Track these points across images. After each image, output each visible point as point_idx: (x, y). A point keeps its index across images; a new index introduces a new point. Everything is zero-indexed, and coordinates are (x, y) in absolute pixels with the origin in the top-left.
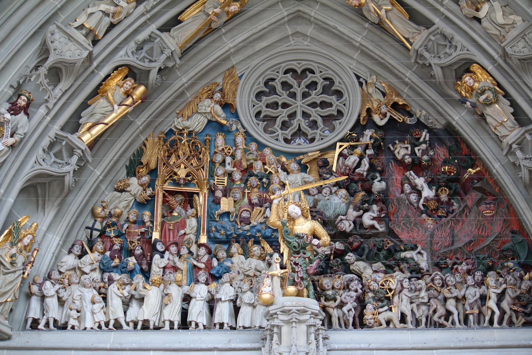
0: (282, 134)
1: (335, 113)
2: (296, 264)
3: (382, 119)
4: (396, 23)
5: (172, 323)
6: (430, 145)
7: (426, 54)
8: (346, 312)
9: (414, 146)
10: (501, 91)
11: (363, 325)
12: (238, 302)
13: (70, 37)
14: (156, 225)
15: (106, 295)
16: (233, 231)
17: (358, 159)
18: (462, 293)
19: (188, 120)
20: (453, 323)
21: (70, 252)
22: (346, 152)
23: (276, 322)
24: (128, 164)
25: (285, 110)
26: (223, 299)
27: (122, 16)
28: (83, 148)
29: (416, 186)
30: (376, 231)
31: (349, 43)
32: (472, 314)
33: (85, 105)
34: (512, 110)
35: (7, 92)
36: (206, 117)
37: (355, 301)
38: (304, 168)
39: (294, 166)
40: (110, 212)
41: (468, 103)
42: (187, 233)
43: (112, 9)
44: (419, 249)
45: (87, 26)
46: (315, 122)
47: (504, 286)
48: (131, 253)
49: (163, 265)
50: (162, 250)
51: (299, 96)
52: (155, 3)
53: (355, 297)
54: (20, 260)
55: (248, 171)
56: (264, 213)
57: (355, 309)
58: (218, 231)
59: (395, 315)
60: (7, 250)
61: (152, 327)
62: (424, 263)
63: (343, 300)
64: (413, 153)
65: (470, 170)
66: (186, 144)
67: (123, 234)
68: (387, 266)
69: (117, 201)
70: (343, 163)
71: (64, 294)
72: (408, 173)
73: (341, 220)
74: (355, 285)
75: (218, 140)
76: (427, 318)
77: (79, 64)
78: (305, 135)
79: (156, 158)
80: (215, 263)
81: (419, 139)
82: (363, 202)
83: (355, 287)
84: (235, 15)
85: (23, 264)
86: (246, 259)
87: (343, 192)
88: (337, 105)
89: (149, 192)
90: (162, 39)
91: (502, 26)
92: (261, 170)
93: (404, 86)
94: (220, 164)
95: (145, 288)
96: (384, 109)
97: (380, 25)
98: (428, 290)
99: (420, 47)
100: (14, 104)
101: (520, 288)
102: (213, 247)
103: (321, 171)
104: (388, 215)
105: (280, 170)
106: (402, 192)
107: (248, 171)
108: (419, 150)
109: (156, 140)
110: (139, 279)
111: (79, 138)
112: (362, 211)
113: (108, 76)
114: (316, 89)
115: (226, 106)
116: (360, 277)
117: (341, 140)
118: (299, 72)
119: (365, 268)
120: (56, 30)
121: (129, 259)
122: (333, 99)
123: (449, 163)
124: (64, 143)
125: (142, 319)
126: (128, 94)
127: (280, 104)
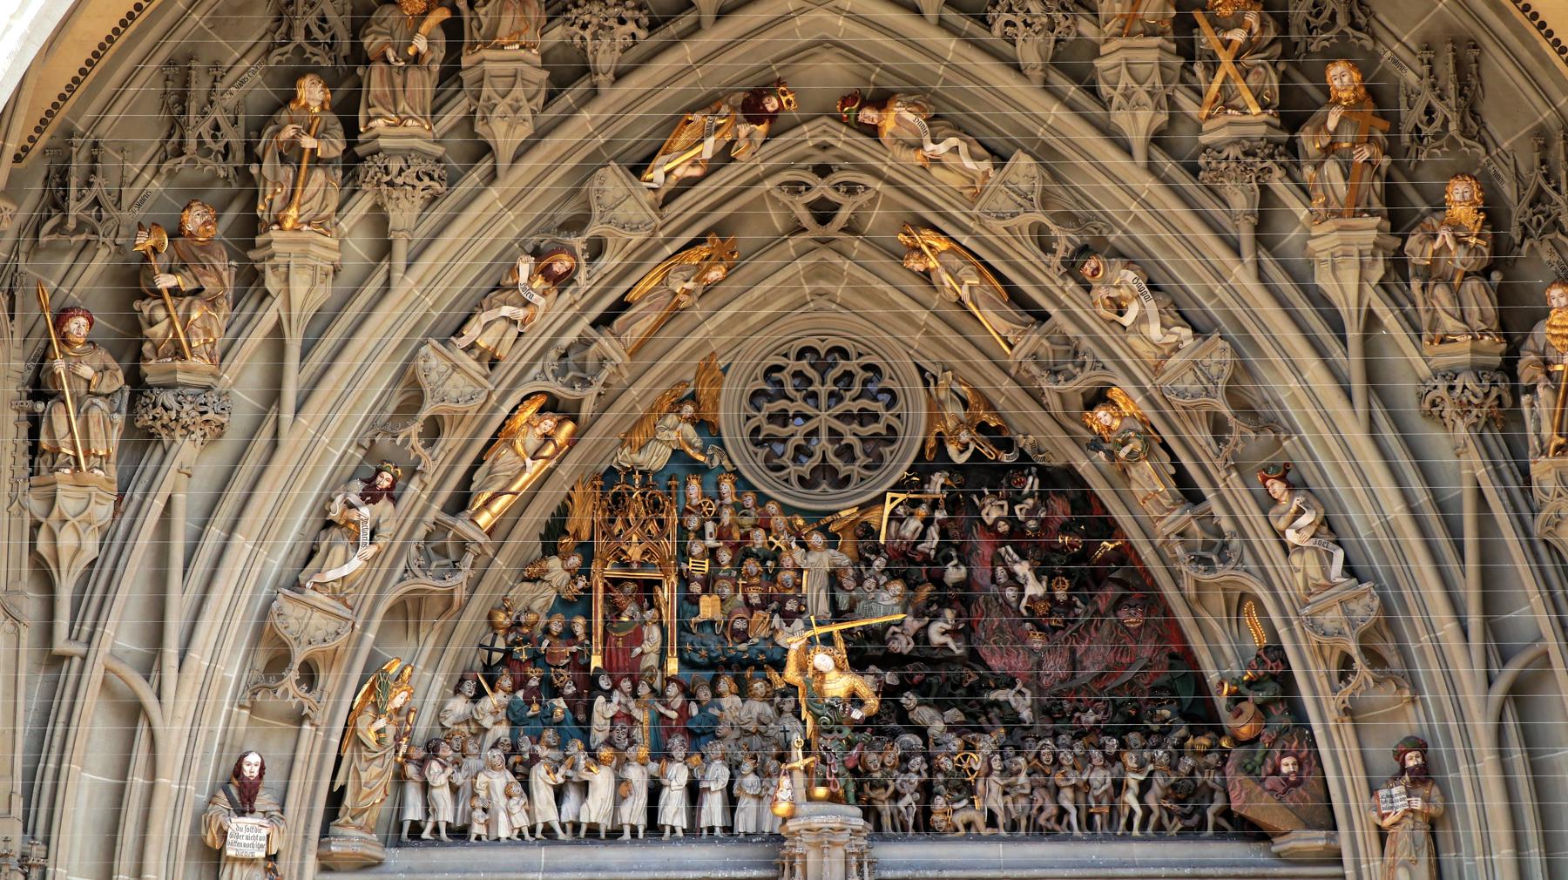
3: (961, 452)
4: (986, 311)
8: (903, 810)
9: (1013, 503)
13: (455, 367)
17: (922, 526)
19: (640, 451)
20: (1069, 826)
22: (901, 510)
24: (543, 532)
26: (713, 789)
30: (950, 654)
31: (908, 318)
35: (353, 455)
38: (832, 540)
39: (817, 539)
40: (518, 617)
43: (521, 313)
44: (1019, 686)
45: (482, 343)
47: (1151, 767)
48: (556, 692)
49: (610, 714)
54: (391, 731)
56: (770, 622)
57: (916, 803)
58: (695, 651)
61: (603, 835)
62: (1026, 714)
63: (899, 787)
65: (1105, 543)
66: (639, 499)
67: (540, 656)
68: (966, 715)
70: (898, 531)
71: (459, 779)
74: (917, 762)
76: (1029, 818)
78: (835, 471)
79: (590, 524)
80: (694, 710)
82: (929, 602)
83: (917, 767)
85: (395, 739)
86: (743, 701)
87: (897, 587)
95: (590, 770)
96: (964, 437)
100: (370, 482)
103: (861, 546)
105: (794, 545)
106: (994, 580)
107: (742, 552)
110: (575, 747)
111: (473, 521)
113: (515, 408)
115: (703, 425)
116: (922, 732)
117: (896, 488)
118: (823, 354)
119: (932, 719)
120: (432, 353)
121: (555, 702)
123: (1071, 530)
126: (547, 438)
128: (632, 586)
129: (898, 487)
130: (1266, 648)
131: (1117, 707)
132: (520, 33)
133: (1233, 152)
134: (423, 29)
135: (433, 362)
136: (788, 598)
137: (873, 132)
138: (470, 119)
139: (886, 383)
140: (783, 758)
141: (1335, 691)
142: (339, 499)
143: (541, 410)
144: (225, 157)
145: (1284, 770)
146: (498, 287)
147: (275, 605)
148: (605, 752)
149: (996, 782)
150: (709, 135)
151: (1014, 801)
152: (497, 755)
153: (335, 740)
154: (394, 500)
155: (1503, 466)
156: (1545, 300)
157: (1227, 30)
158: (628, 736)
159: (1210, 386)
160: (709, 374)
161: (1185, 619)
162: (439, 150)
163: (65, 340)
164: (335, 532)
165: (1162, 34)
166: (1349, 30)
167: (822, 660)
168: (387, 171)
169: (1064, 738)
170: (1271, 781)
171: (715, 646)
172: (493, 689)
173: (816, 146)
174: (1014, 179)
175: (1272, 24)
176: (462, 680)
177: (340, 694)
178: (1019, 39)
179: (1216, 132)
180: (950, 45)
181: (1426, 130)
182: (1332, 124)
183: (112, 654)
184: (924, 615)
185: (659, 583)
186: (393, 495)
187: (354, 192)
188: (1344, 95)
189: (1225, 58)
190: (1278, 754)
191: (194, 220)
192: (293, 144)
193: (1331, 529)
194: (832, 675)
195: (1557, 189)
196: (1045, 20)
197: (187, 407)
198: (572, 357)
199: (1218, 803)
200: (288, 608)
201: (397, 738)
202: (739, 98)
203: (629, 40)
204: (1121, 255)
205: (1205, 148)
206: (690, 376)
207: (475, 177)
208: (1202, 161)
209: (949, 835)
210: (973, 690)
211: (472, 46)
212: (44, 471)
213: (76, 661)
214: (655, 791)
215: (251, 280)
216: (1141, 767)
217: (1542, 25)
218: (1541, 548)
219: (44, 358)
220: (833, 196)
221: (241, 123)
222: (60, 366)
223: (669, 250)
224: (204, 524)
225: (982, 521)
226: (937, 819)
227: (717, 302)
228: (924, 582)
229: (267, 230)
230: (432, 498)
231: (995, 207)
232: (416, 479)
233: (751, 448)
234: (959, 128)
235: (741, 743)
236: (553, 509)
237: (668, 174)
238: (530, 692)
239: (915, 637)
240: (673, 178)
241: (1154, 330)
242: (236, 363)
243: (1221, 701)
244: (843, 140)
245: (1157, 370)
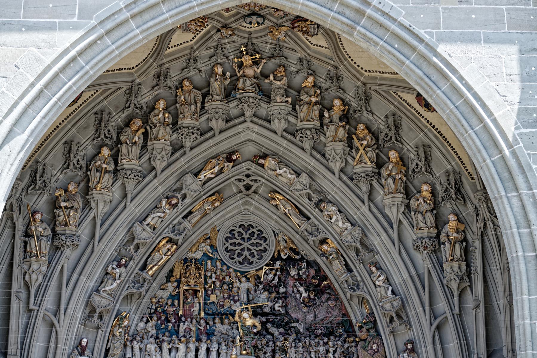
9: (299, 270)
22: (267, 272)
30: (280, 312)
31: (271, 217)
38: (248, 280)
39: (243, 279)
43: (163, 215)
47: (336, 346)
48: (169, 321)
49: (185, 328)
54: (123, 332)
55: (223, 283)
62: (302, 330)
71: (142, 346)
74: (271, 343)
80: (208, 327)
81: (301, 267)
87: (266, 293)
96: (286, 251)
100: (119, 262)
106: (293, 292)
107: (223, 283)
110: (175, 337)
113: (160, 241)
114: (253, 236)
115: (211, 246)
116: (272, 335)
117: (266, 265)
119: (275, 331)
120: (137, 226)
128: (191, 291)
129: (266, 265)
130: (370, 313)
131: (327, 328)
132: (164, 136)
133: (363, 175)
134: (137, 134)
135: (138, 228)
136: (235, 296)
137: (262, 166)
138: (150, 159)
139: (264, 235)
140: (233, 342)
141: (388, 326)
142: (110, 266)
143: (167, 242)
144: (80, 169)
145: (374, 348)
146: (156, 207)
147: (92, 296)
148: (183, 339)
149: (293, 350)
150: (217, 166)
152: (153, 340)
153: (107, 335)
154: (126, 267)
155: (436, 264)
156: (448, 218)
157: (362, 141)
158: (190, 334)
159: (355, 240)
162: (140, 169)
163: (34, 220)
164: (109, 276)
165: (344, 141)
166: (395, 142)
167: (245, 315)
169: (312, 337)
171: (214, 309)
173: (246, 169)
174: (302, 180)
175: (374, 139)
176: (143, 317)
177: (109, 321)
178: (304, 142)
179: (358, 169)
180: (285, 143)
181: (416, 170)
182: (390, 168)
183: (46, 310)
185: (199, 291)
186: (125, 265)
187: (116, 180)
188: (394, 160)
189: (361, 148)
191: (72, 187)
192: (100, 166)
193: (388, 281)
195: (451, 188)
196: (311, 136)
197: (68, 240)
198: (176, 227)
200: (95, 297)
201: (125, 334)
202: (225, 156)
203: (195, 139)
204: (331, 202)
205: (355, 173)
206: (209, 232)
207: (151, 176)
208: (354, 177)
210: (287, 323)
211: (151, 139)
212: (28, 257)
213: (36, 311)
214: (197, 350)
215: (87, 203)
216: (334, 346)
217: (448, 142)
218: (446, 288)
219: (29, 225)
220: (250, 183)
221: (85, 160)
222: (33, 228)
223: (204, 197)
224: (72, 272)
225: (290, 275)
227: (217, 212)
229: (92, 190)
230: (136, 266)
231: (296, 188)
232: (132, 261)
233: (225, 253)
234: (286, 165)
235: (221, 337)
236: (169, 269)
237: (205, 176)
238: (162, 321)
239: (271, 308)
240: (206, 178)
241: (340, 224)
242: (83, 227)
243: (356, 328)
244: (254, 168)
245: (341, 235)
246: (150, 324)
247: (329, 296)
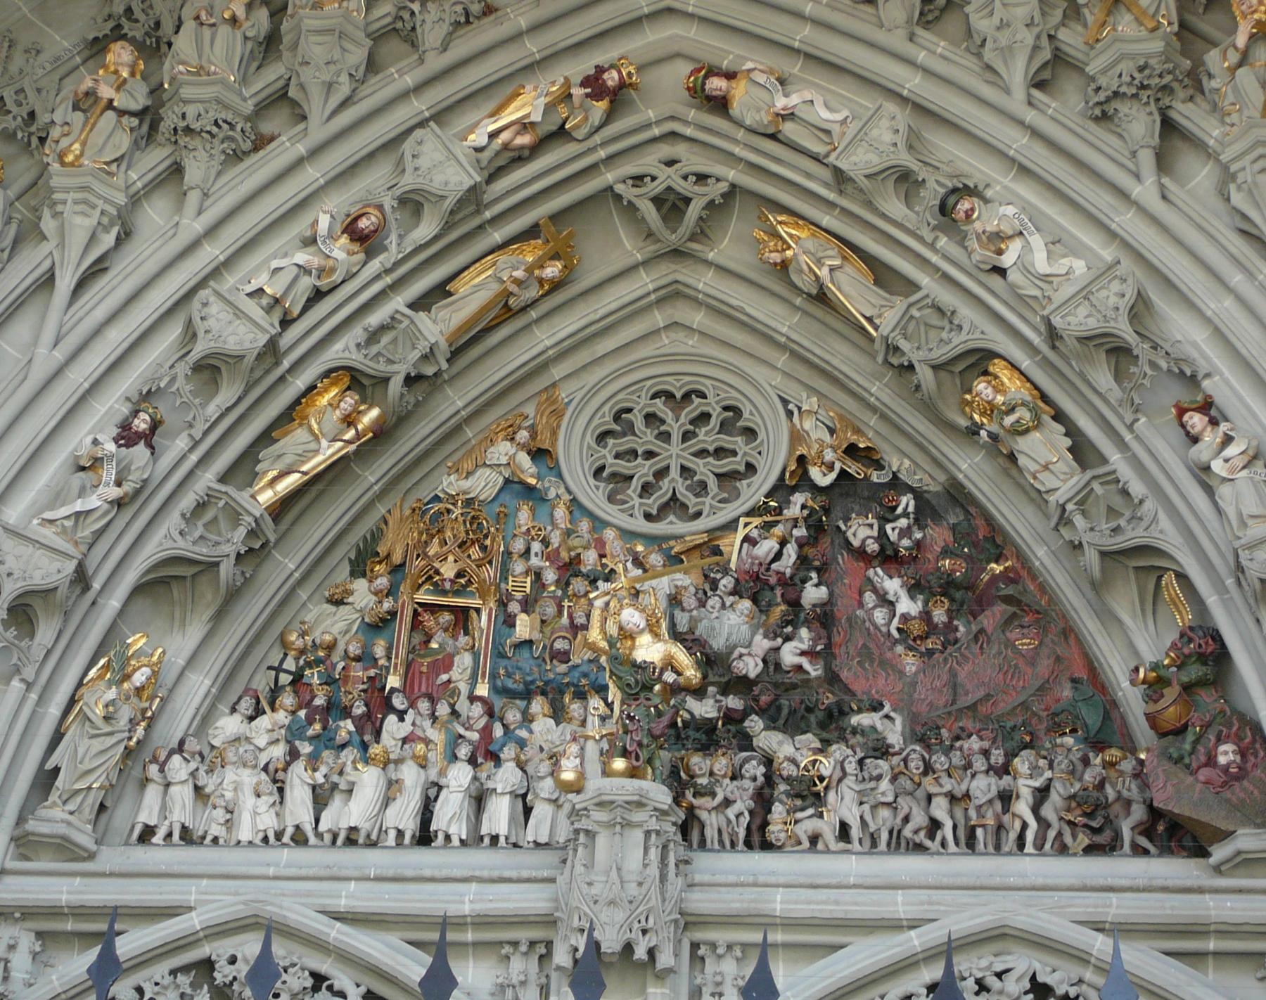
0: (641, 504)
1: (742, 468)
2: (631, 718)
5: (400, 834)
6: (916, 520)
7: (904, 345)
8: (732, 818)
9: (884, 520)
10: (1047, 408)
11: (767, 846)
12: (529, 797)
14: (396, 665)
15: (283, 782)
16: (536, 676)
17: (777, 546)
18: (964, 787)
19: (467, 477)
21: (233, 710)
22: (755, 534)
23: (584, 824)
25: (648, 463)
26: (499, 791)
27: (337, 277)
28: (258, 515)
29: (886, 593)
30: (805, 677)
31: (768, 338)
32: (983, 826)
33: (266, 438)
34: (1068, 442)
36: (501, 473)
37: (751, 799)
38: (674, 560)
39: (655, 559)
41: (983, 433)
42: (454, 679)
44: (887, 708)
45: (268, 291)
46: (703, 485)
47: (1048, 774)
48: (346, 713)
49: (403, 734)
50: (402, 707)
51: (676, 437)
52: (401, 256)
53: (751, 791)
55: (570, 568)
57: (751, 812)
58: (509, 675)
59: (827, 827)
60: (97, 695)
61: (361, 841)
62: (894, 735)
64: (882, 534)
65: (993, 565)
69: (328, 622)
72: (871, 572)
73: (741, 656)
75: (520, 514)
76: (891, 832)
77: (250, 358)
78: (684, 506)
80: (498, 731)
81: (895, 508)
83: (752, 771)
84: (556, 285)
86: (557, 724)
87: (746, 604)
88: (745, 454)
89: (387, 605)
90: (412, 322)
91: (1046, 278)
92: (595, 565)
93: (869, 413)
94: (521, 556)
96: (829, 456)
97: (821, 297)
98: (894, 779)
99: (893, 331)
101: (1081, 779)
102: (498, 703)
104: (829, 646)
105: (629, 565)
106: (861, 605)
107: (570, 568)
108: (893, 529)
109: (407, 512)
112: (780, 640)
113: (312, 387)
115: (538, 454)
117: (749, 514)
118: (678, 395)
119: (780, 743)
121: (342, 724)
122: (738, 442)
124: (221, 503)
125: (346, 826)
126: (349, 421)
127: (640, 452)
137: (720, 105)
149: (849, 789)
151: (874, 808)
159: (1111, 314)
160: (550, 405)
161: (1089, 625)
168: (184, 116)
170: (1204, 774)
172: (273, 710)
184: (776, 636)
190: (1213, 738)
194: (645, 639)
199: (1138, 813)
209: (790, 849)
223: (497, 236)
226: (776, 830)
228: (778, 605)
233: (592, 481)
237: (493, 135)
246: (264, 722)
247: (1011, 609)
